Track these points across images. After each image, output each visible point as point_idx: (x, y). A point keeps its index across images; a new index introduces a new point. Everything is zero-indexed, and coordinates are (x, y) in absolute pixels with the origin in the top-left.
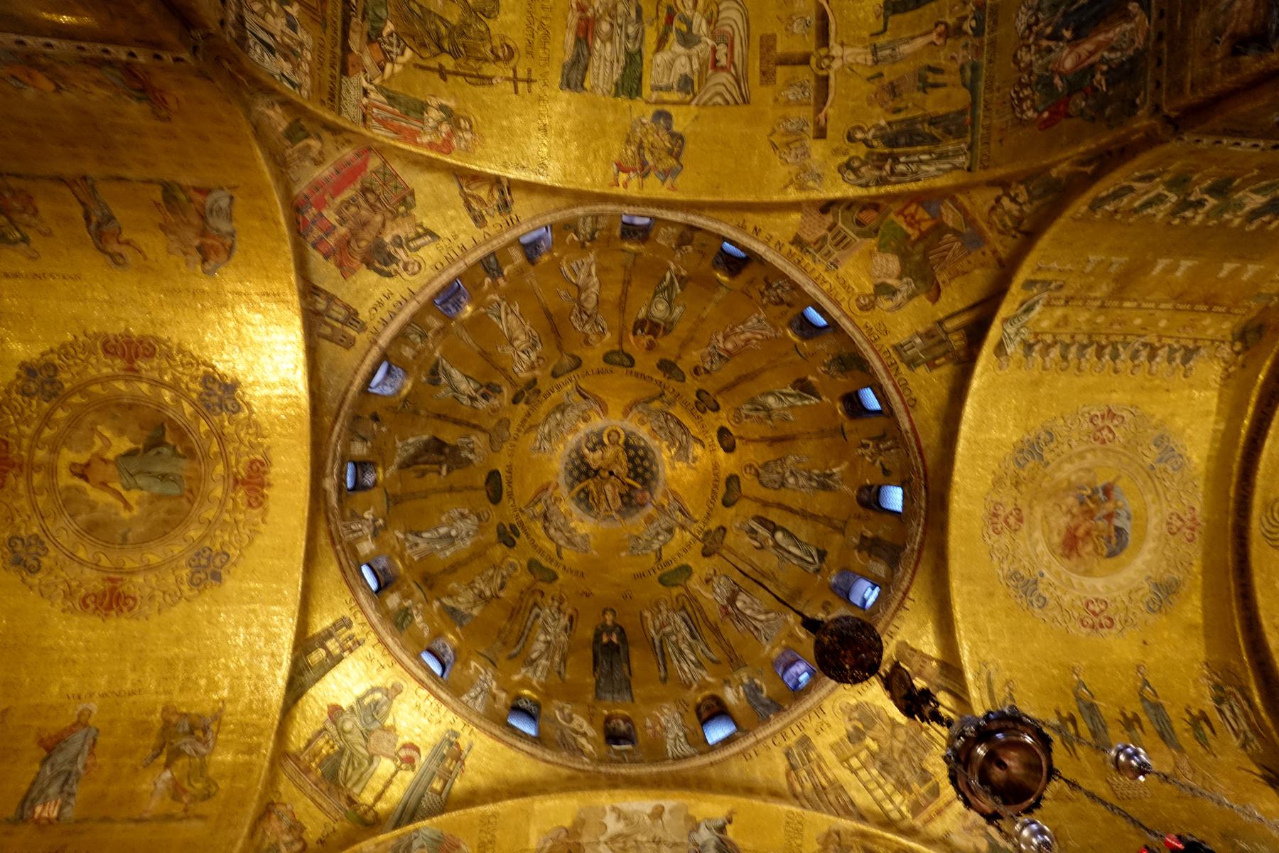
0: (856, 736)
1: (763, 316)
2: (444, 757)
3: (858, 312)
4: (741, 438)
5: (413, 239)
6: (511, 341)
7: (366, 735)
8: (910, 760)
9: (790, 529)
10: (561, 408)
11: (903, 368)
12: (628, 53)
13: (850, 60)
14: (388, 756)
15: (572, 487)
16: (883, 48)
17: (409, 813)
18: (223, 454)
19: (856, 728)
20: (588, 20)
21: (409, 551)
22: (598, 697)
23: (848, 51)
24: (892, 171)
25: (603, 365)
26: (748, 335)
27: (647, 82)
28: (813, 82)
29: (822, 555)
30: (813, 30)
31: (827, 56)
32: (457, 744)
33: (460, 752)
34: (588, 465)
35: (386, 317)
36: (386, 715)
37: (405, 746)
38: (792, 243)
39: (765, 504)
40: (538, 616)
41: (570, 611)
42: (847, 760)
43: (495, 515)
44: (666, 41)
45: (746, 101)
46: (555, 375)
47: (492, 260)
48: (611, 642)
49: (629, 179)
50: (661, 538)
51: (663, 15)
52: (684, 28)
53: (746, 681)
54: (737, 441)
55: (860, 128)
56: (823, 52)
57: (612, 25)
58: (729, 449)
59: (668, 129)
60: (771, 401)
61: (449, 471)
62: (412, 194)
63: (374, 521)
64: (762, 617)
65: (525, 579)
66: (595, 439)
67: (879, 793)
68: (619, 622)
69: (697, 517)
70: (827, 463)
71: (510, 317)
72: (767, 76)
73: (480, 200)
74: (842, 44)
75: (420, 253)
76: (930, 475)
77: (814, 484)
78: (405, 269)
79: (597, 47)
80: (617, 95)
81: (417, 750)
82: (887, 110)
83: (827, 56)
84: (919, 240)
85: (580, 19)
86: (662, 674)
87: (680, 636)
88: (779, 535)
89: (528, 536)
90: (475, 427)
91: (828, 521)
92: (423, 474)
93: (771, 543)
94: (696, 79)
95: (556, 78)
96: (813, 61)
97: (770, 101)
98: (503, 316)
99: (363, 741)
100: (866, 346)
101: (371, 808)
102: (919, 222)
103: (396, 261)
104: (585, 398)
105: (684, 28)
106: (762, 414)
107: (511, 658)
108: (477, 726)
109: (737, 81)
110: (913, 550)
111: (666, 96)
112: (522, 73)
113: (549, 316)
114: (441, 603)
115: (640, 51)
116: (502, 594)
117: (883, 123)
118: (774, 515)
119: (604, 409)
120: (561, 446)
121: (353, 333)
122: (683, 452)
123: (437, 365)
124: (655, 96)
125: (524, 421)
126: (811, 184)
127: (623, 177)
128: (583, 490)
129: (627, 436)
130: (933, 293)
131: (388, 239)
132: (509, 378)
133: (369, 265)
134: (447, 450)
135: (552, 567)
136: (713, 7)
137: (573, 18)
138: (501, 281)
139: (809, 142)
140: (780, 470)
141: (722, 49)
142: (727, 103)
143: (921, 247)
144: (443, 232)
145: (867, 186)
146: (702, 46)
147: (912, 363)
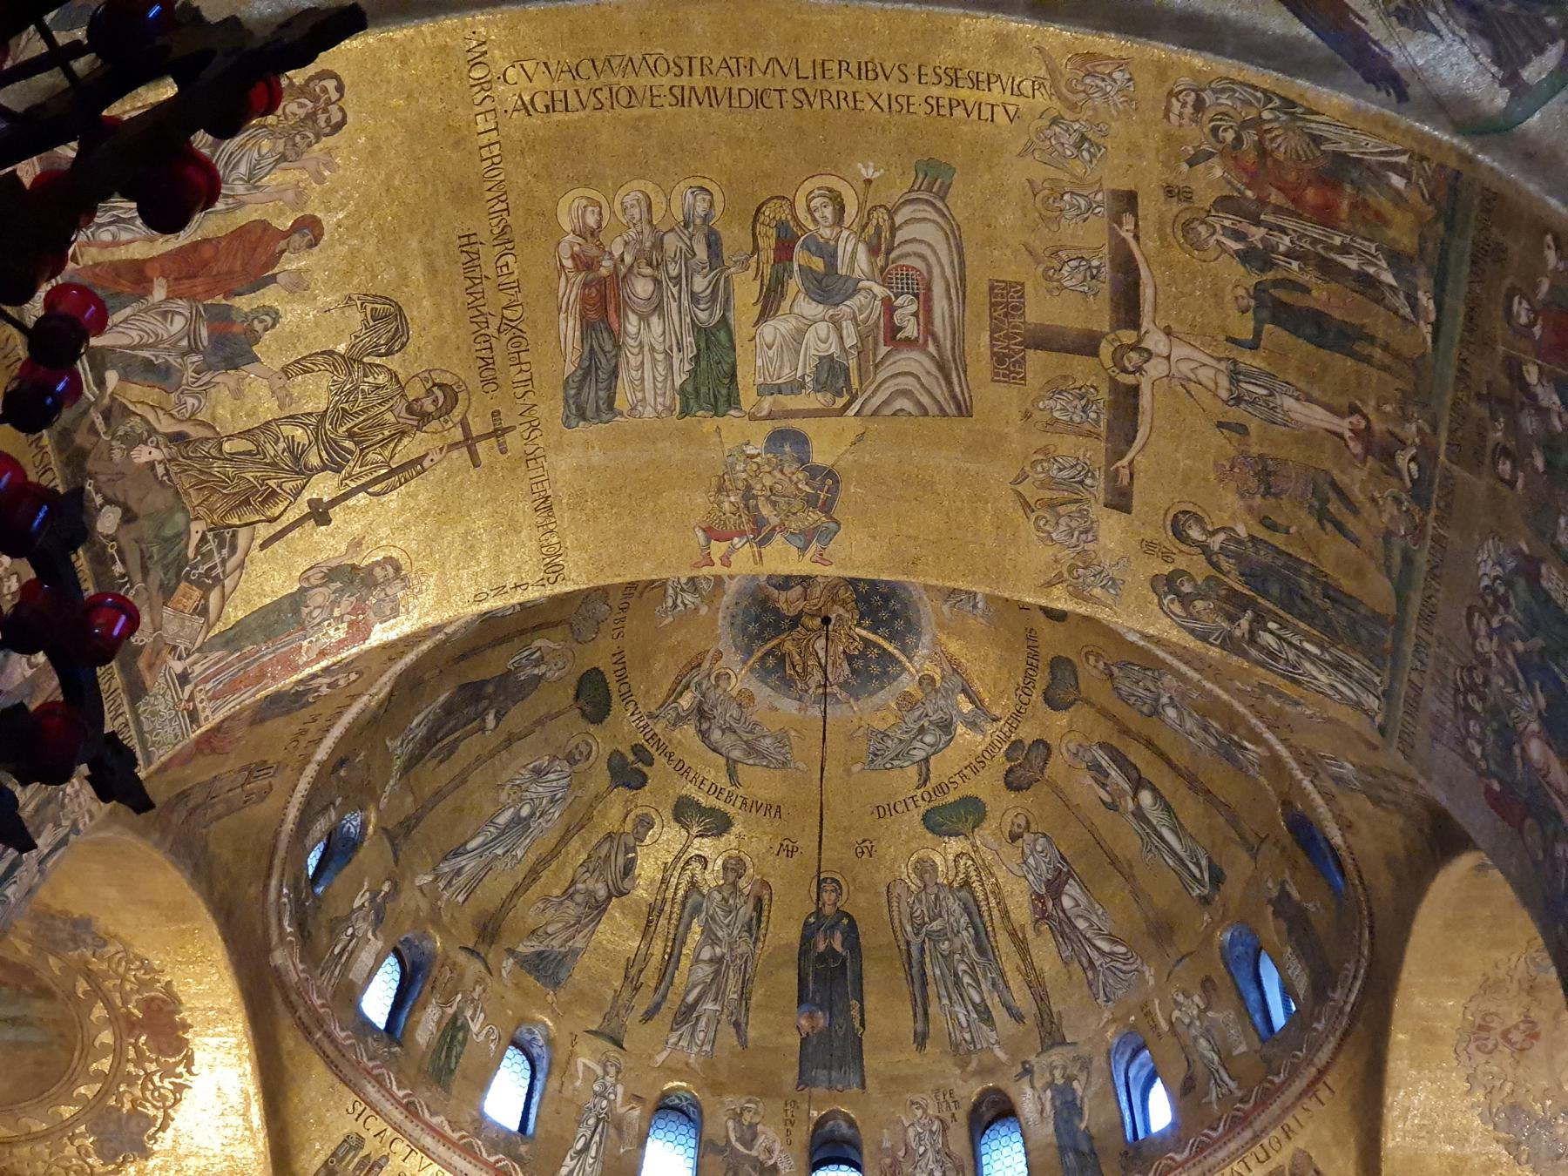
12: (698, 329)
13: (1185, 368)
16: (1251, 377)
18: (97, 992)
20: (603, 281)
21: (446, 895)
22: (804, 1081)
23: (1180, 351)
24: (1252, 639)
27: (747, 379)
28: (1104, 394)
29: (1217, 878)
30: (1105, 288)
31: (1135, 347)
34: (776, 611)
39: (1125, 731)
43: (602, 742)
44: (783, 296)
45: (964, 411)
48: (831, 950)
49: (733, 550)
50: (929, 739)
51: (768, 243)
52: (818, 264)
55: (1199, 520)
56: (1128, 337)
57: (657, 282)
59: (803, 461)
61: (498, 718)
68: (846, 909)
69: (997, 712)
72: (1006, 366)
74: (1168, 332)
79: (632, 329)
80: (685, 412)
83: (1135, 347)
85: (585, 285)
88: (1146, 797)
89: (670, 756)
92: (452, 750)
93: (1131, 805)
94: (852, 364)
95: (551, 409)
96: (1106, 349)
97: (1016, 415)
105: (818, 264)
109: (942, 367)
111: (791, 402)
112: (476, 428)
115: (724, 320)
117: (1242, 531)
118: (1139, 756)
124: (767, 403)
126: (1097, 591)
127: (718, 548)
128: (769, 653)
135: (720, 804)
136: (880, 216)
137: (569, 290)
139: (1096, 510)
141: (906, 307)
142: (926, 413)
145: (1204, 637)
146: (860, 299)
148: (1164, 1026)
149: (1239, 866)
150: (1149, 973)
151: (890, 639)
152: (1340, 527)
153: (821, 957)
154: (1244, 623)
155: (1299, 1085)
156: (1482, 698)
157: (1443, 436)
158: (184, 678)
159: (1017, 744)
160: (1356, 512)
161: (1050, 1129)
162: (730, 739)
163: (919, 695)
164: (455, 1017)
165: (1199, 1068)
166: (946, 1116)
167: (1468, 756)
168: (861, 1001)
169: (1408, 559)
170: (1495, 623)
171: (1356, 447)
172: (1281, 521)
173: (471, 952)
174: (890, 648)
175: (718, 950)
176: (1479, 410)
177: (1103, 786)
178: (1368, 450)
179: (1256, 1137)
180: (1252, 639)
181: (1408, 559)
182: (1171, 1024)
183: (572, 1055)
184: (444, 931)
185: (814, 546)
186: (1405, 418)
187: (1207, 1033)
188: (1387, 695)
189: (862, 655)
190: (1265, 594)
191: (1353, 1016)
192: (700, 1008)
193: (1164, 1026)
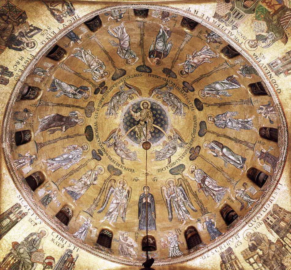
0: (253, 248)
1: (209, 48)
2: (65, 262)
3: (250, 49)
4: (206, 104)
5: (29, 32)
6: (90, 66)
7: (30, 254)
8: (276, 259)
9: (230, 147)
10: (119, 94)
11: (273, 74)
14: (41, 263)
19: (253, 244)
25: (137, 72)
26: (204, 56)
32: (72, 256)
33: (73, 259)
34: (134, 119)
35: (22, 68)
36: (39, 245)
37: (47, 258)
38: (214, 17)
39: (218, 135)
40: (112, 192)
41: (128, 188)
42: (248, 259)
46: (113, 79)
47: (72, 34)
48: (147, 202)
50: (170, 152)
53: (207, 220)
54: (204, 105)
58: (200, 109)
60: (218, 86)
61: (66, 129)
62: (24, 12)
63: (31, 157)
64: (217, 189)
65: (107, 175)
66: (136, 107)
68: (151, 193)
70: (245, 116)
71: (87, 56)
73: (58, 10)
75: (34, 37)
76: (289, 125)
77: (240, 126)
78: (28, 46)
84: (274, 14)
86: (170, 217)
87: (179, 198)
88: (225, 150)
89: (107, 155)
90: (77, 107)
91: (246, 143)
92: (54, 131)
98: (83, 56)
99: (28, 257)
100: (254, 64)
102: (273, 5)
103: (23, 43)
104: (130, 88)
106: (214, 92)
107: (99, 212)
108: (80, 247)
110: (282, 161)
113: (106, 53)
114: (66, 190)
116: (95, 182)
118: (222, 140)
119: (140, 93)
120: (120, 111)
121: (7, 78)
122: (177, 110)
123: (54, 82)
125: (101, 101)
128: (132, 131)
129: (152, 105)
130: (284, 39)
131: (16, 34)
132: (91, 83)
133: (10, 47)
134: (64, 119)
135: (119, 168)
138: (79, 41)
140: (224, 119)
143: (275, 17)
144: (43, 27)
147: (278, 73)
148: (234, 199)
162: (122, 153)
164: (49, 195)
166: (178, 234)
175: (118, 202)
177: (214, 152)
182: (236, 198)
187: (246, 195)
189: (154, 132)
192: (113, 213)
193: (234, 199)
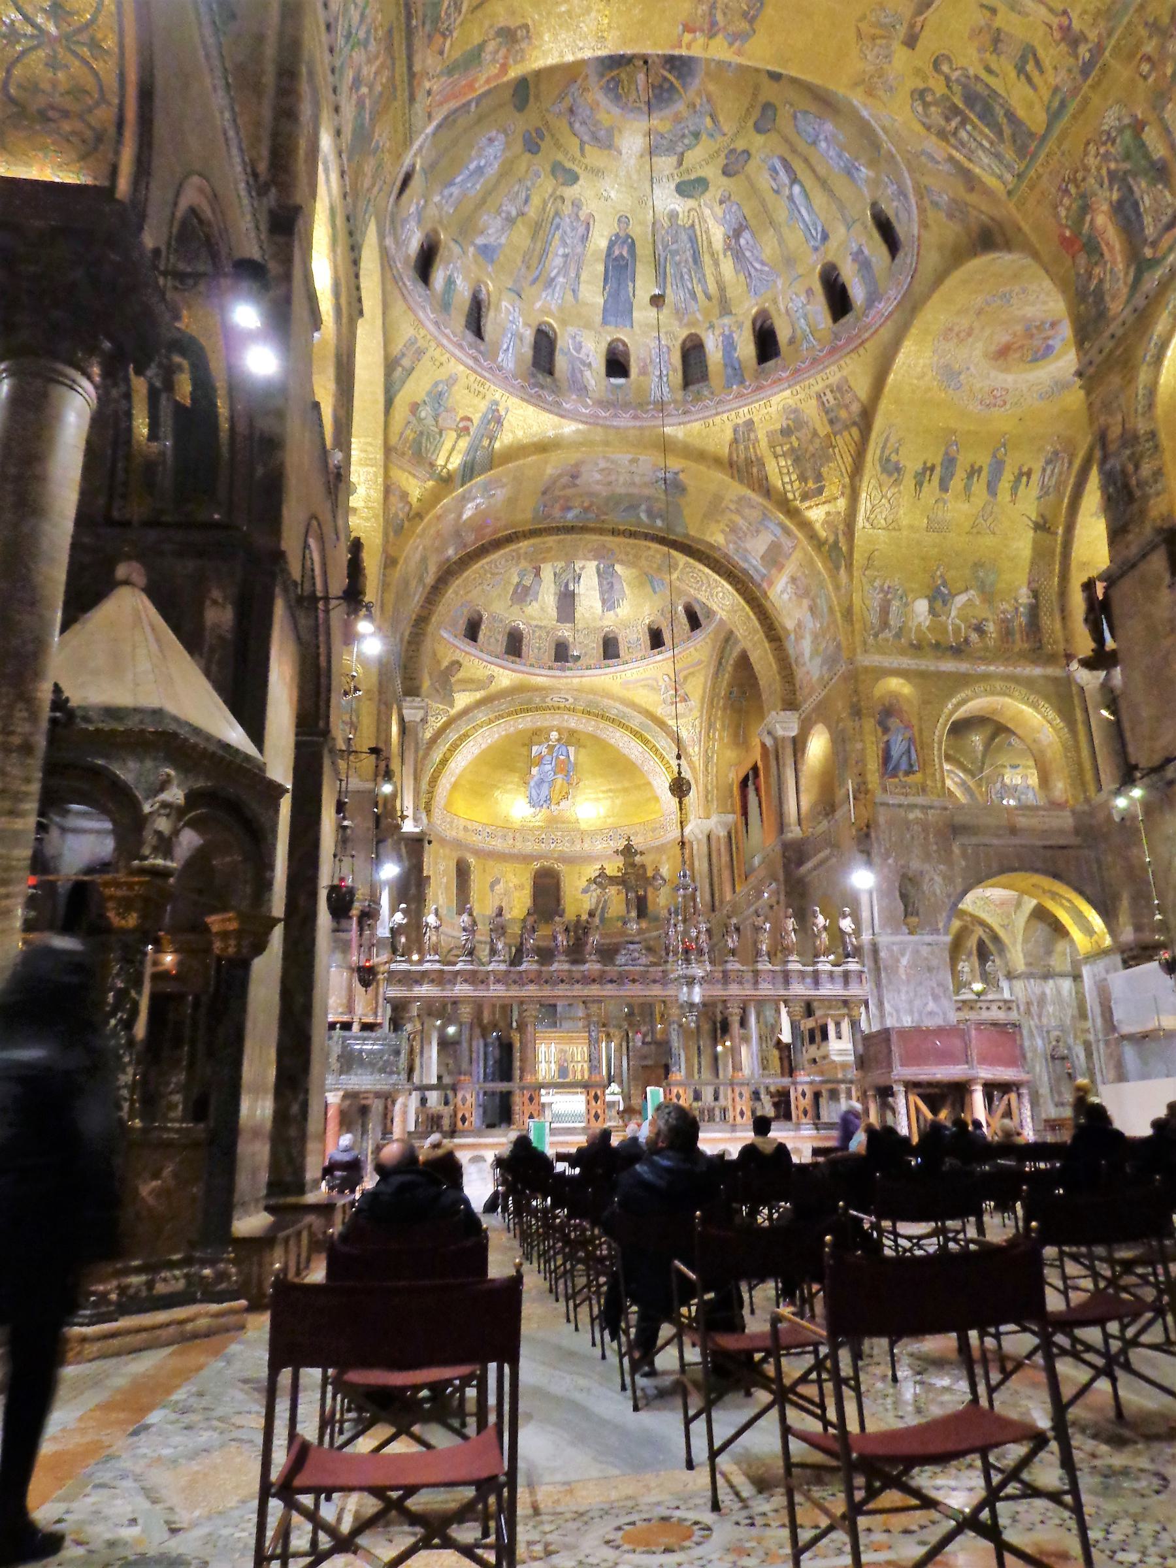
0: (786, 432)
15: (602, 76)
17: (469, 471)
22: (605, 322)
29: (825, 237)
37: (462, 419)
48: (621, 256)
49: (694, 40)
50: (686, 141)
64: (758, 266)
67: (787, 479)
81: (469, 419)
82: (981, 60)
88: (797, 189)
89: (553, 136)
101: (445, 466)
117: (971, 72)
127: (687, 37)
128: (613, 78)
149: (839, 233)
150: (780, 282)
151: (678, 78)
152: (1029, 80)
153: (616, 259)
154: (954, 124)
155: (852, 346)
156: (1077, 187)
157: (1113, 42)
158: (429, 93)
159: (733, 151)
160: (1042, 71)
161: (720, 354)
163: (685, 114)
165: (799, 332)
167: (1056, 215)
168: (634, 281)
169: (1063, 105)
170: (1102, 150)
171: (1057, 35)
172: (994, 66)
173: (456, 241)
174: (676, 83)
176: (1143, 32)
178: (1063, 39)
179: (826, 367)
180: (955, 134)
181: (1063, 105)
183: (500, 300)
184: (446, 229)
185: (737, 44)
186: (1094, 24)
187: (805, 316)
188: (1020, 176)
189: (661, 87)
190: (972, 108)
191: (888, 318)
